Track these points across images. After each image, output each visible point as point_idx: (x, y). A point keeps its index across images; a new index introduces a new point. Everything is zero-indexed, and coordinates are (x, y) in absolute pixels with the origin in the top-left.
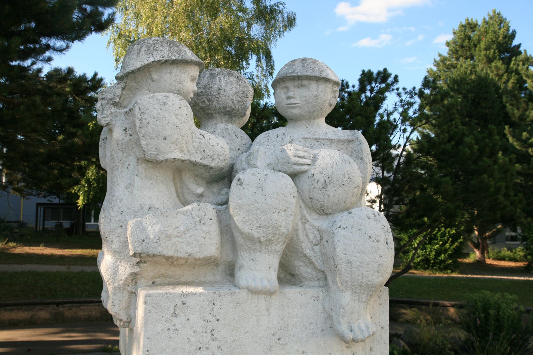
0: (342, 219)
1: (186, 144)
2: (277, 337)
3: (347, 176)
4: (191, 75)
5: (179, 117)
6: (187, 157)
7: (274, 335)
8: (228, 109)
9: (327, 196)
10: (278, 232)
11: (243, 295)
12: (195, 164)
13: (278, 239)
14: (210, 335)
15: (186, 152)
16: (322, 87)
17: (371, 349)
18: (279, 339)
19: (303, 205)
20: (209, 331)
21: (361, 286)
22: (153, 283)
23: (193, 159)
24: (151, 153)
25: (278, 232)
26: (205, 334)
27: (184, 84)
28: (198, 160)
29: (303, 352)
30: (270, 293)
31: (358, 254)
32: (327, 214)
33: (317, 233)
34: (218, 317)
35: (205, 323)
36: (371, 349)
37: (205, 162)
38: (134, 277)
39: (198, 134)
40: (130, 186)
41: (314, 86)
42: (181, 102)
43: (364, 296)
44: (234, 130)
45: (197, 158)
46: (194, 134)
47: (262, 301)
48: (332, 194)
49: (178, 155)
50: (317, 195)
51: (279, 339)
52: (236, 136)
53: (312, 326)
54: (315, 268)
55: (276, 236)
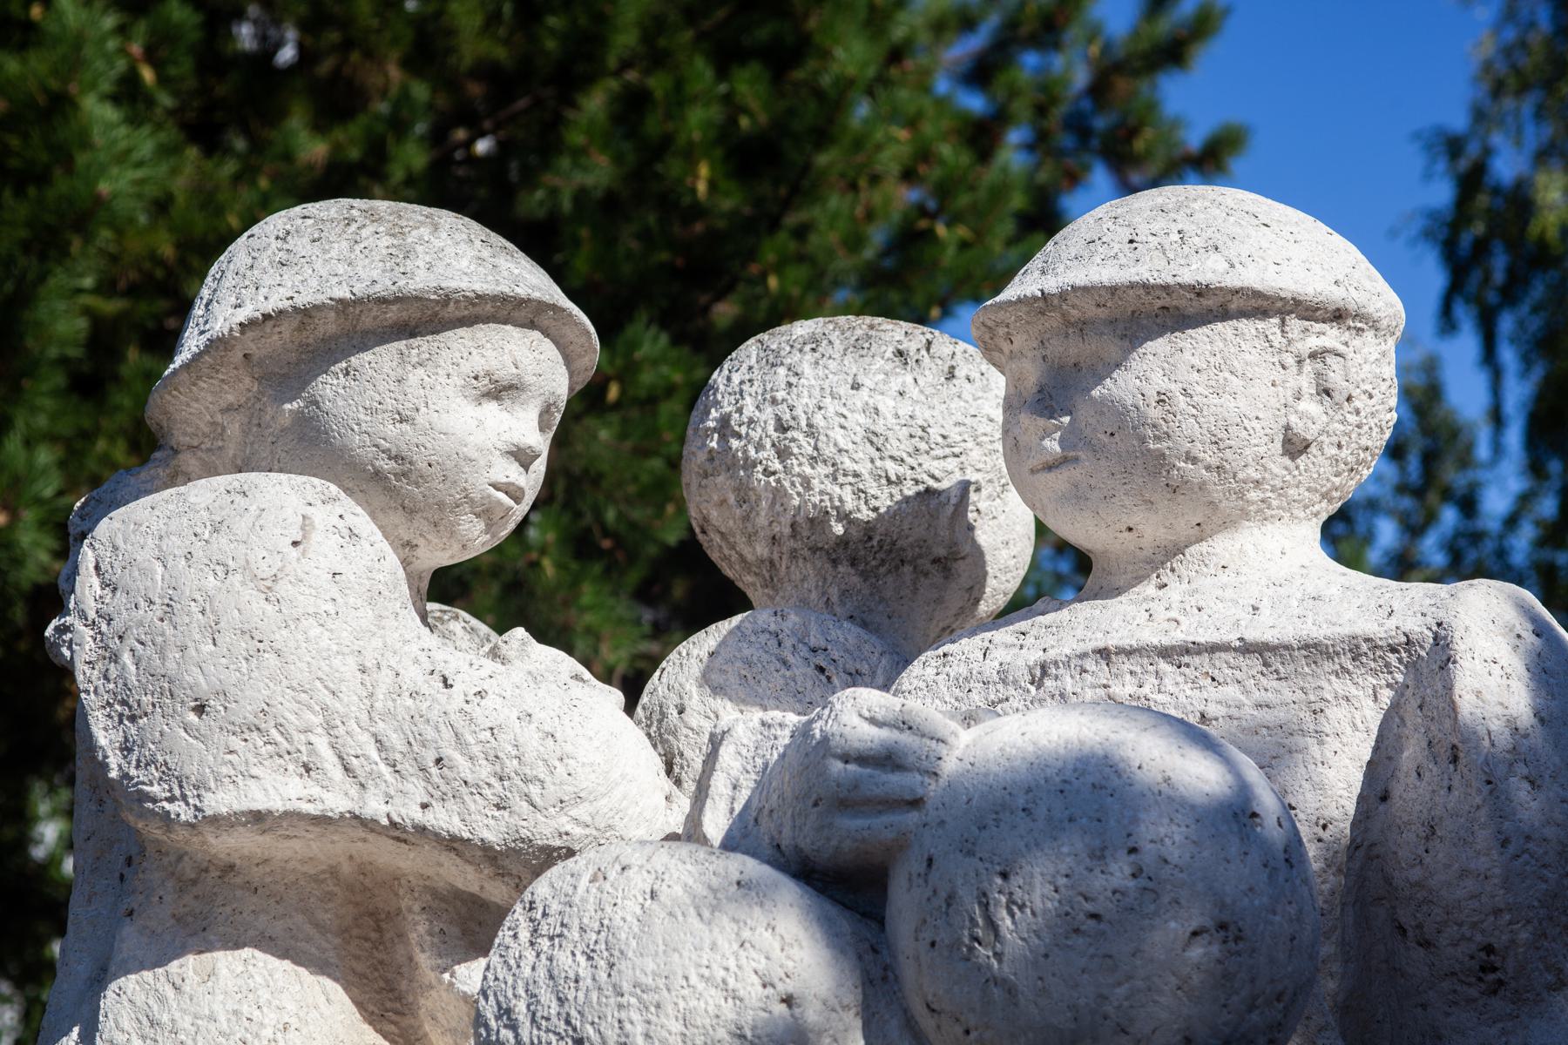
1: (329, 727)
4: (466, 368)
5: (284, 589)
6: (337, 801)
8: (839, 529)
9: (997, 993)
15: (337, 773)
23: (375, 807)
27: (420, 419)
28: (409, 812)
37: (444, 819)
42: (322, 516)
44: (815, 639)
46: (386, 677)
52: (821, 670)
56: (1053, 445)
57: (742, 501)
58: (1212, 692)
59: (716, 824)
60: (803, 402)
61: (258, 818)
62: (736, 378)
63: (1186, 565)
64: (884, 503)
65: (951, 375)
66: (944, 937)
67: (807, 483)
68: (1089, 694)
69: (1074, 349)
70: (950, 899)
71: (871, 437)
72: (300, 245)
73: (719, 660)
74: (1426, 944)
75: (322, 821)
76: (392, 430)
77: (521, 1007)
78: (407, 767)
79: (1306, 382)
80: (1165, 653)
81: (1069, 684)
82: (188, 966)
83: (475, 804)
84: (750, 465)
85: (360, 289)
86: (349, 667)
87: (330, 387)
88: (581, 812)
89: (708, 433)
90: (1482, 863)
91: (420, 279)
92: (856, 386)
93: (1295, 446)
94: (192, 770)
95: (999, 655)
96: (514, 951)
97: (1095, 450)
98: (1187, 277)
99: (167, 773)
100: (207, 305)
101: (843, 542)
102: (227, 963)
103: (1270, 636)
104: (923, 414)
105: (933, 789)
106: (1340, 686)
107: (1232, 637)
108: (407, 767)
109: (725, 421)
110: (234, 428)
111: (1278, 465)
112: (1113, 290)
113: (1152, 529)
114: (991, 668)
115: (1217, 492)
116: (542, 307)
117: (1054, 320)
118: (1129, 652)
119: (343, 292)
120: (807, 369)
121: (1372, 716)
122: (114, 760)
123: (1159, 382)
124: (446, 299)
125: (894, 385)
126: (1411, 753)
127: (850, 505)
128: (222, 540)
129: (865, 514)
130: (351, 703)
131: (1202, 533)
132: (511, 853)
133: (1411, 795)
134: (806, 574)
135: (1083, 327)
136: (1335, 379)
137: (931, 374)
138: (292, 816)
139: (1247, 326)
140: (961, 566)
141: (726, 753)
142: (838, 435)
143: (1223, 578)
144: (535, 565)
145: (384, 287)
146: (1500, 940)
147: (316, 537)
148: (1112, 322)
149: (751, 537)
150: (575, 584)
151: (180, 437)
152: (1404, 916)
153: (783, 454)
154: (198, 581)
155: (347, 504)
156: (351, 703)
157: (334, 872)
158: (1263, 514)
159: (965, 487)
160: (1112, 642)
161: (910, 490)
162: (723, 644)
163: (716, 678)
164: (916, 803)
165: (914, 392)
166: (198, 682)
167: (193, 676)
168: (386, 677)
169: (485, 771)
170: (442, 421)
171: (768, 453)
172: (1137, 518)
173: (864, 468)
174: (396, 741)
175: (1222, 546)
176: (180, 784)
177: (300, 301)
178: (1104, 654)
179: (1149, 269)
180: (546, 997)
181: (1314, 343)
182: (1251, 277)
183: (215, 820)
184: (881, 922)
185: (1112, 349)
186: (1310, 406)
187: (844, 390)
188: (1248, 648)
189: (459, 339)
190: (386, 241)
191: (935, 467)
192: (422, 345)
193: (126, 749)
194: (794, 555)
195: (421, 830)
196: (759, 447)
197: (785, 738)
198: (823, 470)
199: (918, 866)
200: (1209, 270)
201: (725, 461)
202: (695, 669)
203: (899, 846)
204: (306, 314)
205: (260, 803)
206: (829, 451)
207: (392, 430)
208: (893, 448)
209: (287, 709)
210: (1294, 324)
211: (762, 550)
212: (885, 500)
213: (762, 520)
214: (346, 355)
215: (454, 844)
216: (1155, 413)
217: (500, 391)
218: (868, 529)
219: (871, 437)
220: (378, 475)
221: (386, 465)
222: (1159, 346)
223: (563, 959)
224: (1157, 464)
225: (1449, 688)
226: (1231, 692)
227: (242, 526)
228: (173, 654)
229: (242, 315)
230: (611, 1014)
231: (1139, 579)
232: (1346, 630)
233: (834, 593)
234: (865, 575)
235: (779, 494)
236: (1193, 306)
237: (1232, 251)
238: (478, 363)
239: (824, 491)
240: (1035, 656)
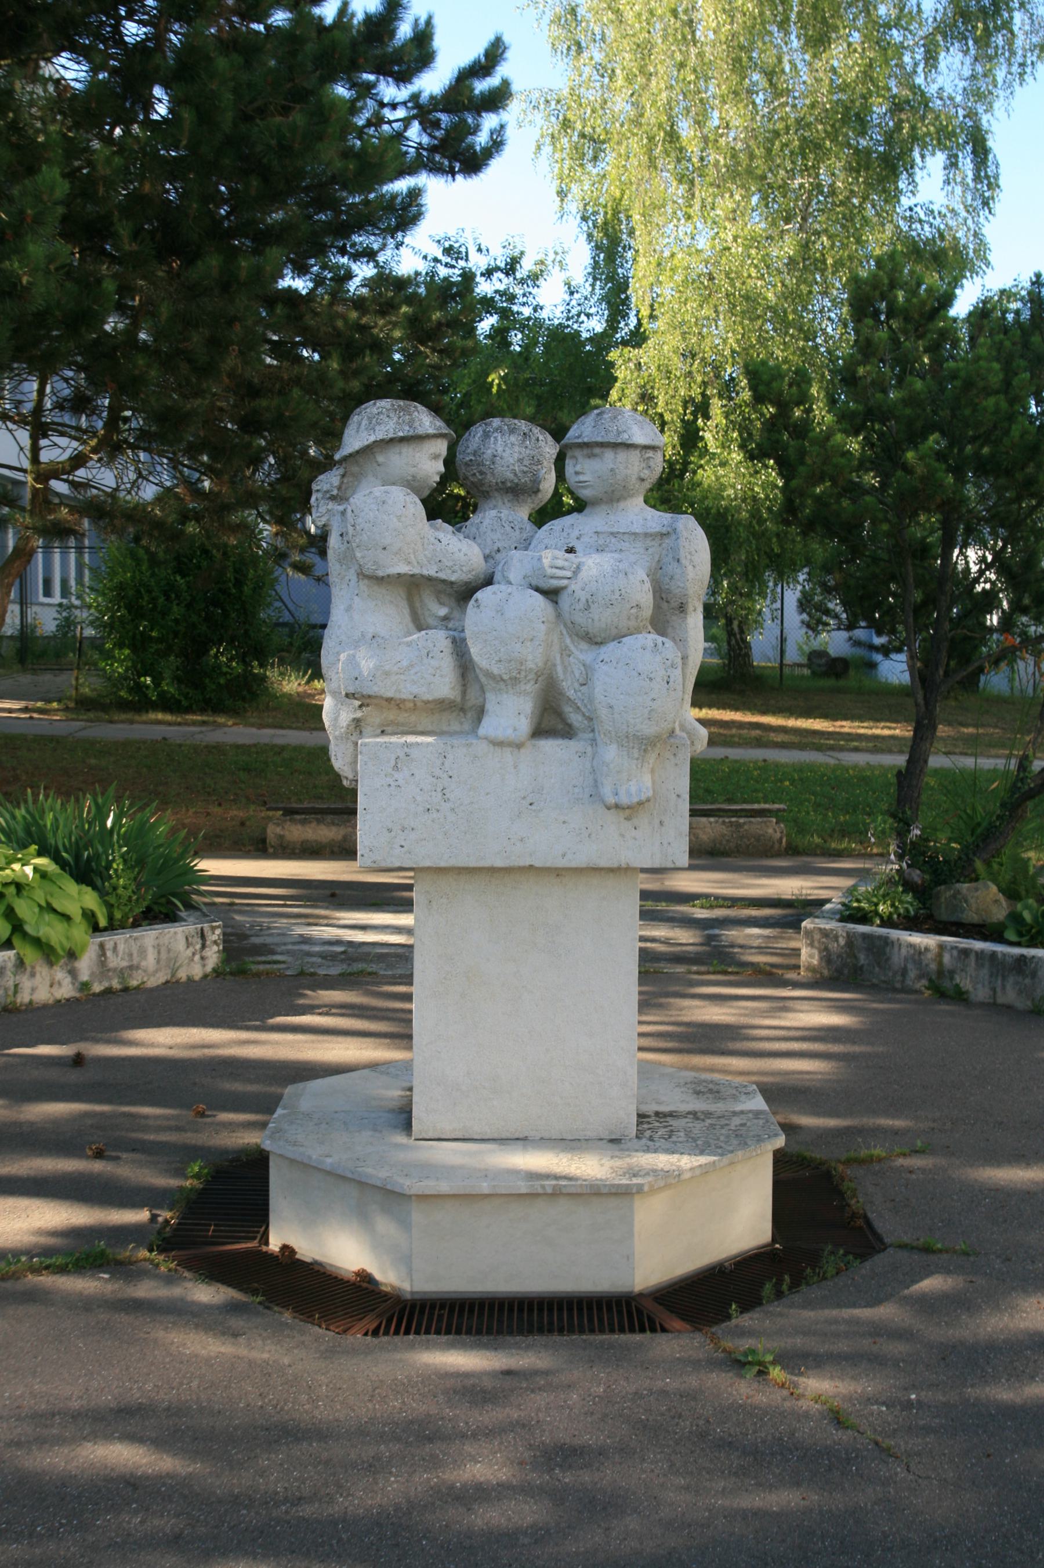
0: (609, 650)
3: (618, 593)
5: (403, 519)
6: (416, 571)
7: (524, 798)
10: (523, 668)
11: (481, 747)
12: (429, 579)
13: (526, 677)
14: (440, 794)
16: (622, 455)
17: (661, 823)
18: (531, 804)
20: (439, 790)
21: (627, 737)
22: (383, 732)
23: (425, 572)
24: (369, 568)
25: (523, 668)
26: (434, 793)
29: (564, 822)
30: (519, 746)
31: (622, 697)
32: (596, 643)
33: (582, 668)
35: (434, 780)
36: (661, 823)
37: (442, 576)
38: (357, 723)
39: (432, 540)
40: (349, 609)
41: (609, 454)
42: (408, 498)
43: (636, 751)
44: (511, 519)
45: (431, 571)
46: (426, 540)
47: (508, 754)
48: (596, 618)
49: (403, 569)
50: (580, 618)
51: (531, 804)
53: (576, 790)
54: (584, 715)
55: (523, 674)
74: (668, 602)
79: (644, 465)
91: (420, 431)
152: (664, 596)
158: (632, 496)
181: (647, 455)
184: (557, 603)
217: (436, 457)
227: (390, 502)
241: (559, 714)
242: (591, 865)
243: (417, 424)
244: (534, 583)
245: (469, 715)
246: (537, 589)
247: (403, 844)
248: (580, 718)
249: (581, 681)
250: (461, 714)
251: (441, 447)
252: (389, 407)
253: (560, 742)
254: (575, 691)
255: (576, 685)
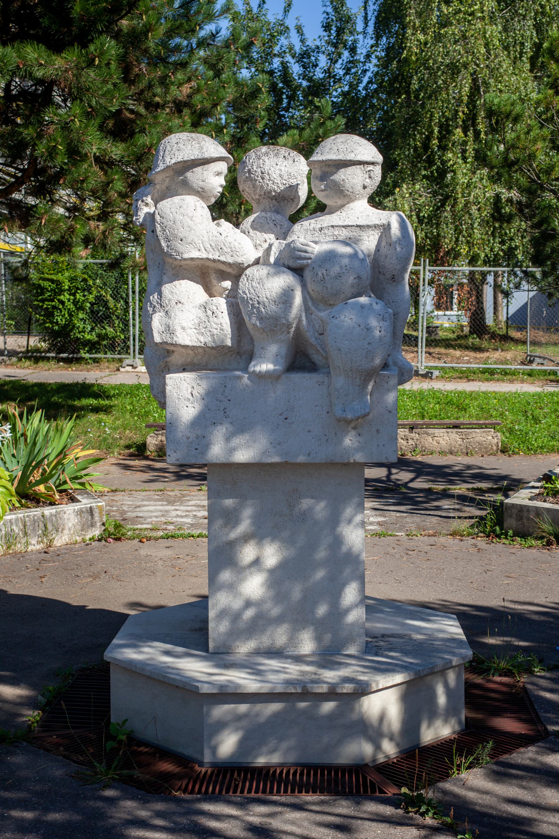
2: (285, 417)
3: (344, 268)
4: (214, 171)
5: (194, 218)
6: (204, 255)
7: (281, 414)
13: (281, 329)
15: (204, 250)
16: (350, 170)
17: (378, 431)
18: (286, 419)
19: (308, 297)
20: (221, 409)
23: (211, 257)
26: (218, 412)
28: (216, 257)
29: (309, 431)
32: (330, 305)
33: (320, 323)
34: (229, 398)
36: (378, 431)
37: (222, 258)
39: (215, 233)
42: (197, 204)
44: (273, 219)
46: (211, 234)
51: (286, 419)
53: (317, 408)
54: (322, 356)
55: (278, 327)
56: (323, 187)
57: (254, 187)
58: (351, 233)
59: (272, 260)
60: (267, 168)
61: (192, 259)
62: (251, 161)
63: (346, 208)
64: (283, 188)
65: (294, 161)
66: (316, 280)
67: (268, 185)
68: (330, 234)
69: (327, 169)
70: (317, 274)
71: (280, 176)
72: (181, 145)
73: (255, 223)
75: (202, 259)
76: (201, 183)
77: (247, 291)
78: (216, 249)
79: (367, 176)
80: (343, 227)
81: (326, 231)
82: (176, 283)
83: (228, 256)
84: (256, 180)
85: (196, 157)
86: (205, 232)
87: (189, 174)
88: (245, 257)
89: (246, 173)
90: (393, 262)
91: (207, 155)
92: (277, 165)
93: (365, 187)
94: (180, 251)
95: (313, 225)
96: (244, 283)
97: (331, 189)
98: (348, 159)
99: (176, 251)
100: (163, 157)
101: (274, 196)
102: (182, 282)
103: (361, 224)
104: (290, 170)
105: (312, 256)
106: (372, 232)
107: (355, 224)
108: (216, 249)
109: (249, 170)
110: (167, 180)
111: (362, 191)
112: (335, 160)
113: (340, 202)
114: (311, 228)
115: (352, 196)
116: (226, 157)
117: (324, 164)
118: (337, 226)
119: (193, 158)
120: (266, 160)
121: (377, 237)
122: (165, 248)
123: (343, 177)
124: (211, 158)
125: (284, 164)
126: (383, 244)
127: (276, 189)
128: (182, 210)
129: (279, 191)
130: (206, 239)
131: (348, 203)
132: (234, 264)
133: (384, 251)
134: (266, 203)
135: (329, 166)
136: (372, 175)
137: (291, 162)
138: (198, 258)
139: (358, 167)
140: (296, 200)
141: (273, 248)
142: (274, 175)
143: (352, 211)
144: (73, 121)
145: (200, 157)
146: (395, 274)
147: (198, 208)
148: (334, 165)
149: (255, 195)
150: (86, 126)
151: (156, 182)
152: (381, 270)
153: (263, 179)
154: (179, 217)
155: (201, 202)
156: (206, 239)
157: (198, 266)
158: (359, 199)
159: (298, 184)
160: (334, 224)
161: (287, 186)
162: (255, 218)
163: (255, 226)
164: (310, 259)
165: (288, 165)
166: (181, 235)
167: (180, 234)
168: (211, 234)
169: (229, 250)
170: (210, 181)
171: (259, 178)
172: (337, 200)
173: (279, 182)
174: (213, 245)
175: (351, 205)
176: (178, 253)
177: (185, 159)
178: (332, 226)
179: (341, 157)
180: (252, 290)
181: (369, 169)
182: (359, 158)
183: (185, 259)
185: (334, 170)
186: (368, 180)
187: (275, 165)
188: (357, 226)
189: (212, 165)
190: (198, 145)
191: (292, 181)
192: (206, 166)
193: (168, 246)
194: (264, 198)
195: (219, 260)
196: (258, 177)
197: (284, 246)
198: (271, 182)
199: (311, 269)
200: (351, 157)
201: (249, 179)
202: (250, 223)
203: (308, 265)
204: (185, 162)
205: (192, 256)
206: (272, 178)
207: (201, 183)
208: (285, 178)
209: (196, 240)
210: (366, 166)
211: (257, 197)
212: (283, 188)
213: (258, 191)
214: (192, 169)
215: (224, 263)
216: (342, 183)
217: (219, 174)
218: (279, 193)
219: (280, 176)
220: (198, 192)
221: (200, 190)
222: (343, 170)
223: (254, 284)
224: (342, 192)
225: (390, 233)
226: (355, 233)
227: (185, 207)
228: (176, 231)
229: (173, 161)
230: (264, 293)
231: (337, 211)
232: (373, 223)
233: (271, 205)
234: (278, 202)
235: (262, 186)
236: (349, 163)
237: (356, 152)
238: (216, 170)
239: (271, 186)
240: (320, 226)
241: (306, 356)
242: (329, 461)
243: (204, 150)
244: (286, 263)
245: (244, 357)
246: (289, 268)
247: (197, 447)
248: (320, 358)
249: (320, 331)
250: (238, 356)
251: (223, 167)
252: (185, 138)
253: (307, 375)
254: (316, 339)
255: (317, 334)
